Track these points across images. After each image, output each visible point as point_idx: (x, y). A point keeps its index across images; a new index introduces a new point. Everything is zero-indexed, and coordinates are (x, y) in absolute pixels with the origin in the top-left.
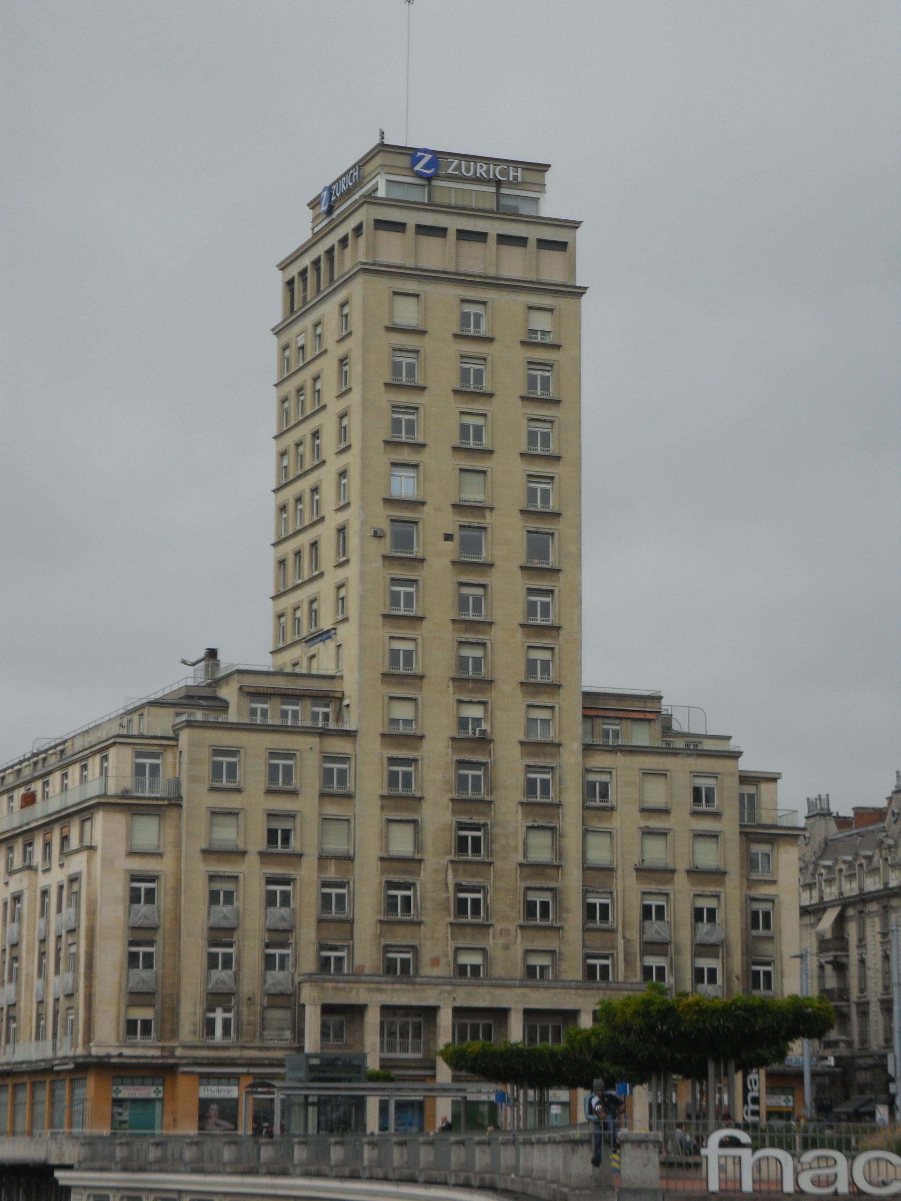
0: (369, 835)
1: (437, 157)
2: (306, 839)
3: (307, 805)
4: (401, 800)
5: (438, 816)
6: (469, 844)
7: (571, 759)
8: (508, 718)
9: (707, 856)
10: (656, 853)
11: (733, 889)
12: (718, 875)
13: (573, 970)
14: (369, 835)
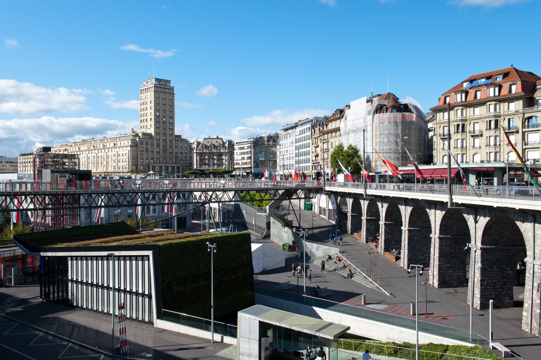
0: (156, 149)
1: (160, 80)
2: (150, 150)
3: (149, 146)
4: (158, 145)
5: (161, 147)
6: (165, 151)
7: (174, 142)
8: (168, 138)
9: (186, 151)
10: (181, 151)
11: (189, 154)
12: (187, 153)
13: (174, 162)
14: (156, 149)
